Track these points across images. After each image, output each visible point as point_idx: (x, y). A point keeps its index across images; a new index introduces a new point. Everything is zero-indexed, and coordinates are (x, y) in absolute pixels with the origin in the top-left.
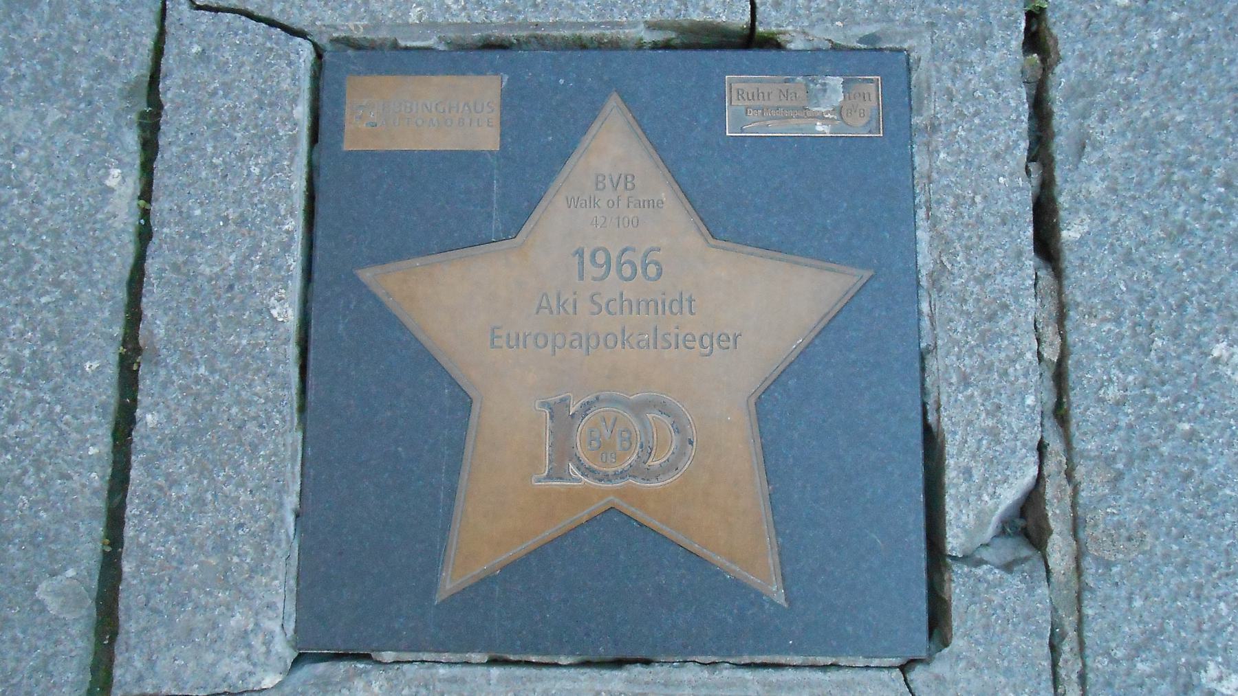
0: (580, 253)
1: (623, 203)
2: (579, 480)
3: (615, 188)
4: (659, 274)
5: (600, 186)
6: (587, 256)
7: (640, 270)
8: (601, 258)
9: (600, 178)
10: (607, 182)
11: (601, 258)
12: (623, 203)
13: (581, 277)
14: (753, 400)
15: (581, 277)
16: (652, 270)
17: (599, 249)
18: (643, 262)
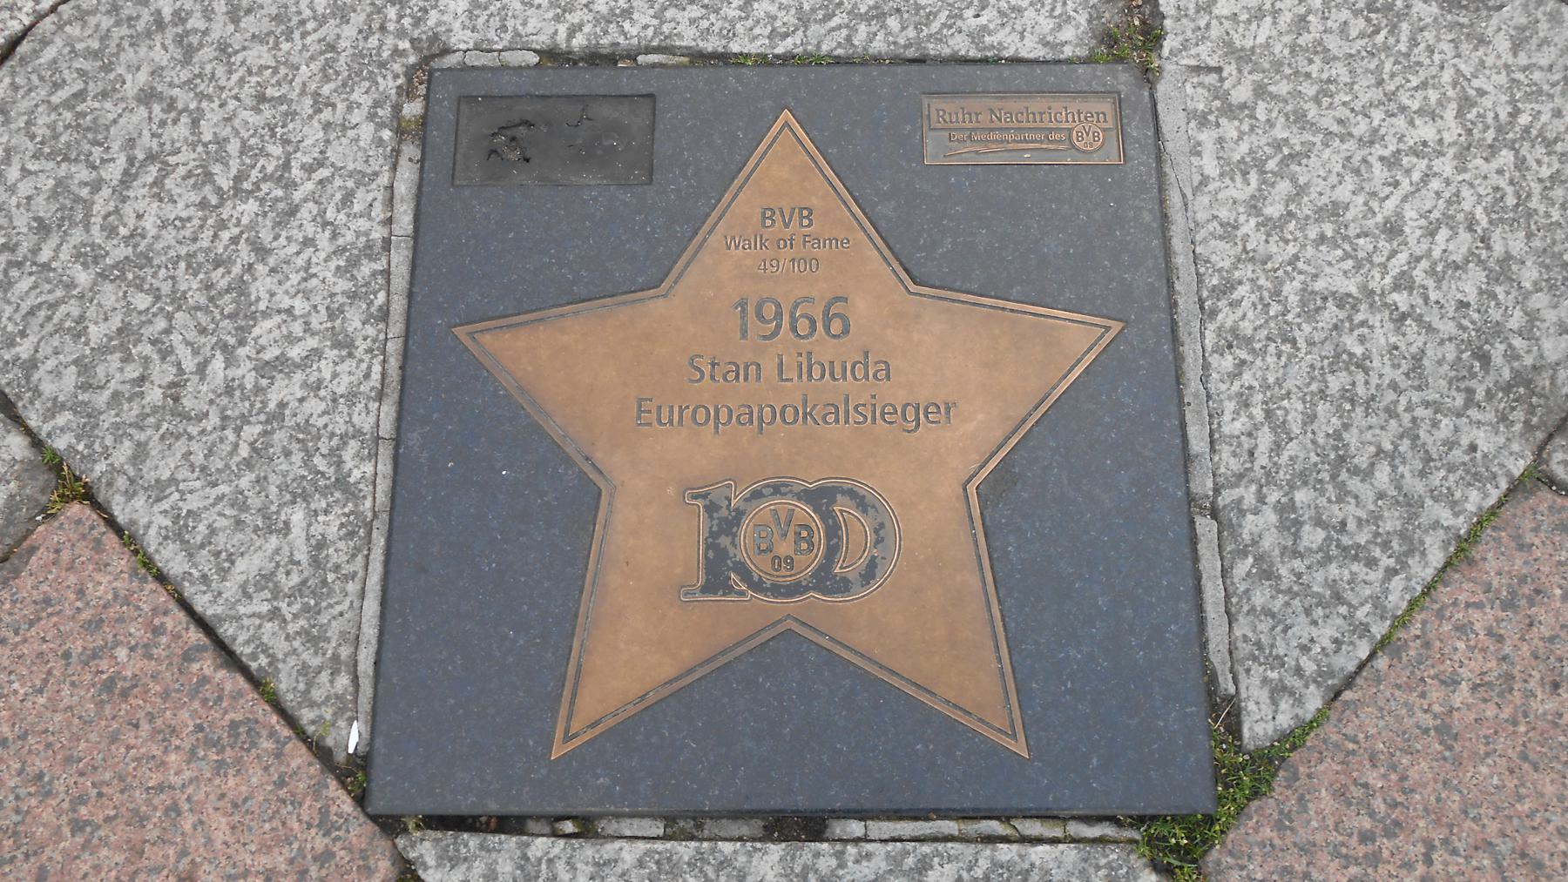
0: (743, 304)
1: (798, 240)
2: (742, 593)
3: (787, 226)
4: (846, 331)
5: (768, 222)
6: (750, 309)
7: (819, 325)
8: (769, 310)
9: (768, 213)
10: (777, 217)
11: (769, 310)
12: (798, 240)
13: (744, 334)
14: (972, 488)
15: (744, 334)
16: (836, 327)
17: (769, 299)
18: (826, 312)
